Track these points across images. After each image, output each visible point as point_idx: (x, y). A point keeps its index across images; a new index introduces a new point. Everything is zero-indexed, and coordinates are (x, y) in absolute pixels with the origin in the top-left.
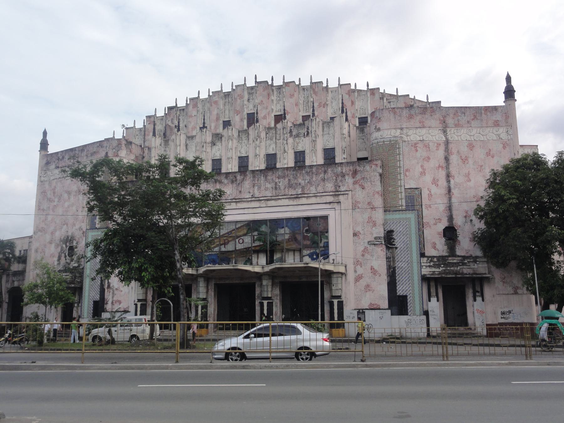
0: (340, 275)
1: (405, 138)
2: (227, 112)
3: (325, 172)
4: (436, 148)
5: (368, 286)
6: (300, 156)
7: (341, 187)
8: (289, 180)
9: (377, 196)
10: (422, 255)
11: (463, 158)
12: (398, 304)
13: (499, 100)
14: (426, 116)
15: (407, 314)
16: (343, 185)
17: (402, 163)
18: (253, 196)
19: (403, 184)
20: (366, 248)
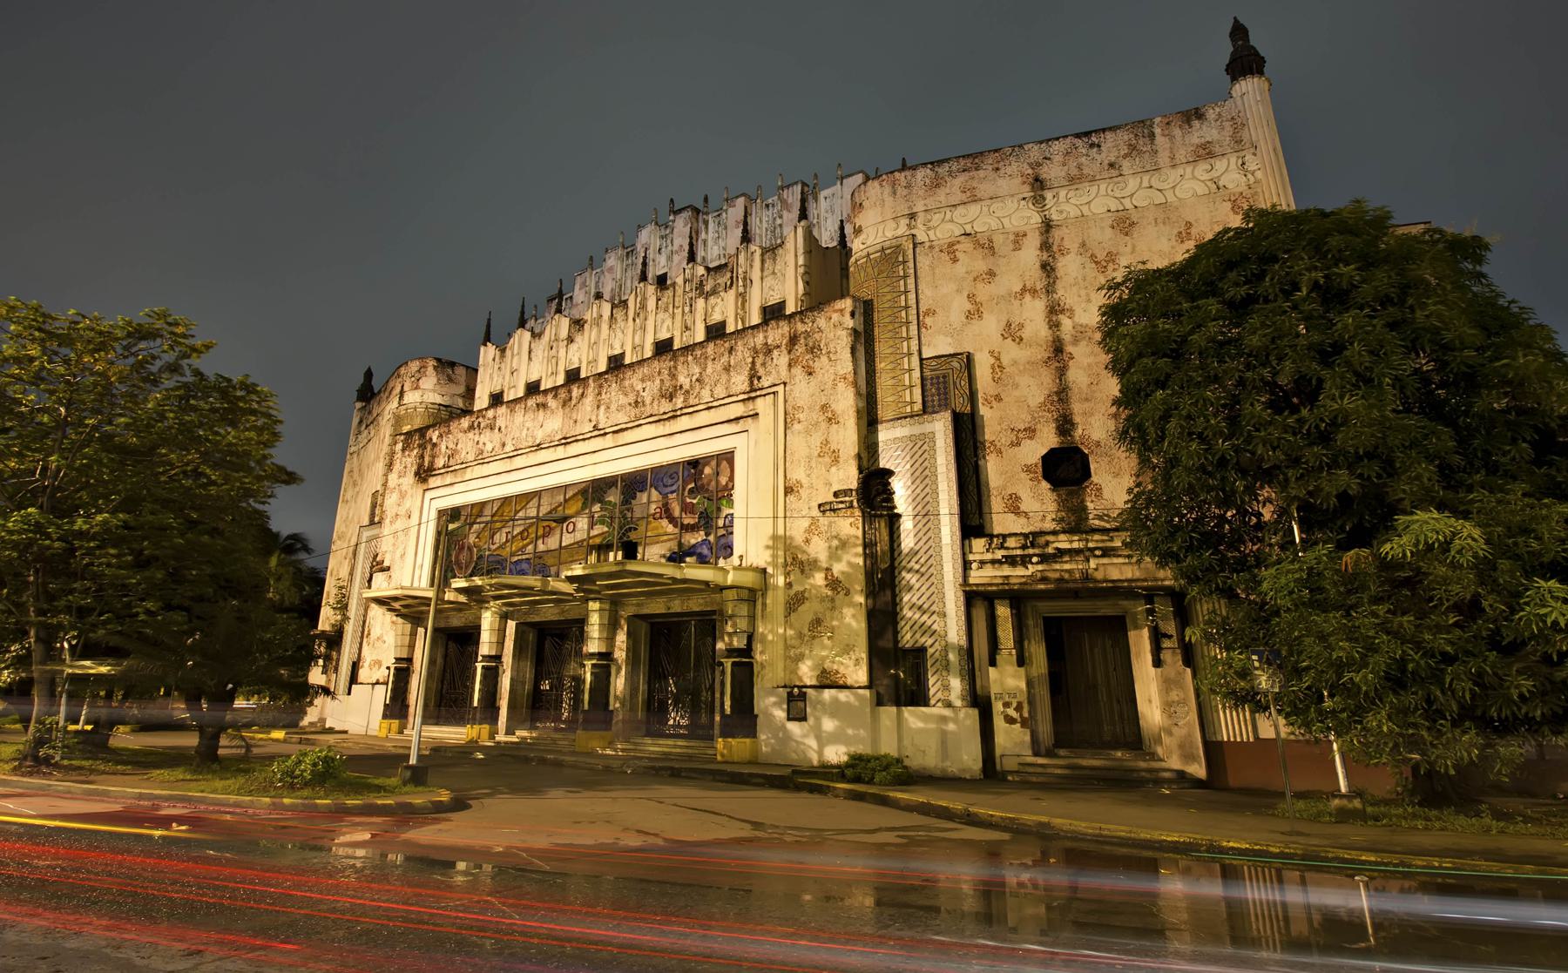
11: (1101, 256)
18: (596, 428)
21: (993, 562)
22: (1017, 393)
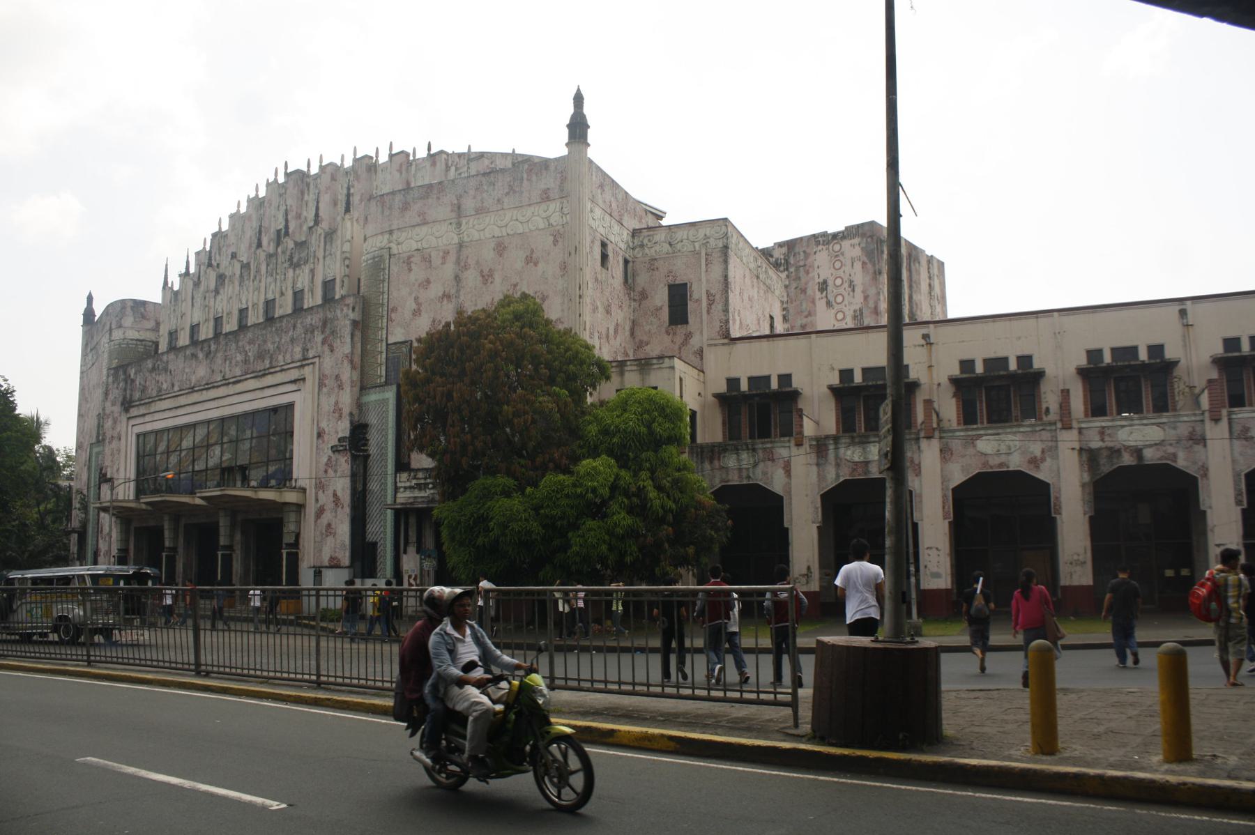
3: (294, 327)
5: (329, 525)
11: (486, 272)
13: (554, 145)
21: (411, 488)
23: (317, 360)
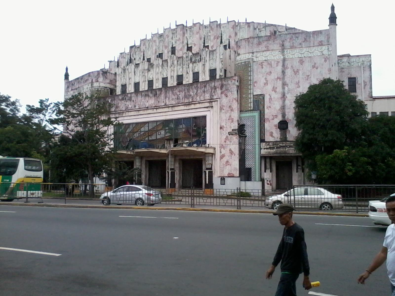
0: (211, 155)
1: (255, 59)
2: (161, 47)
3: (205, 86)
4: (276, 65)
5: (227, 162)
6: (196, 75)
7: (214, 96)
8: (185, 93)
9: (234, 101)
10: (262, 140)
11: (295, 70)
12: (245, 174)
13: (325, 25)
14: (270, 42)
15: (251, 181)
16: (215, 95)
17: (252, 77)
18: (165, 105)
19: (252, 92)
20: (227, 137)
21: (267, 148)
22: (274, 106)
23: (219, 100)
